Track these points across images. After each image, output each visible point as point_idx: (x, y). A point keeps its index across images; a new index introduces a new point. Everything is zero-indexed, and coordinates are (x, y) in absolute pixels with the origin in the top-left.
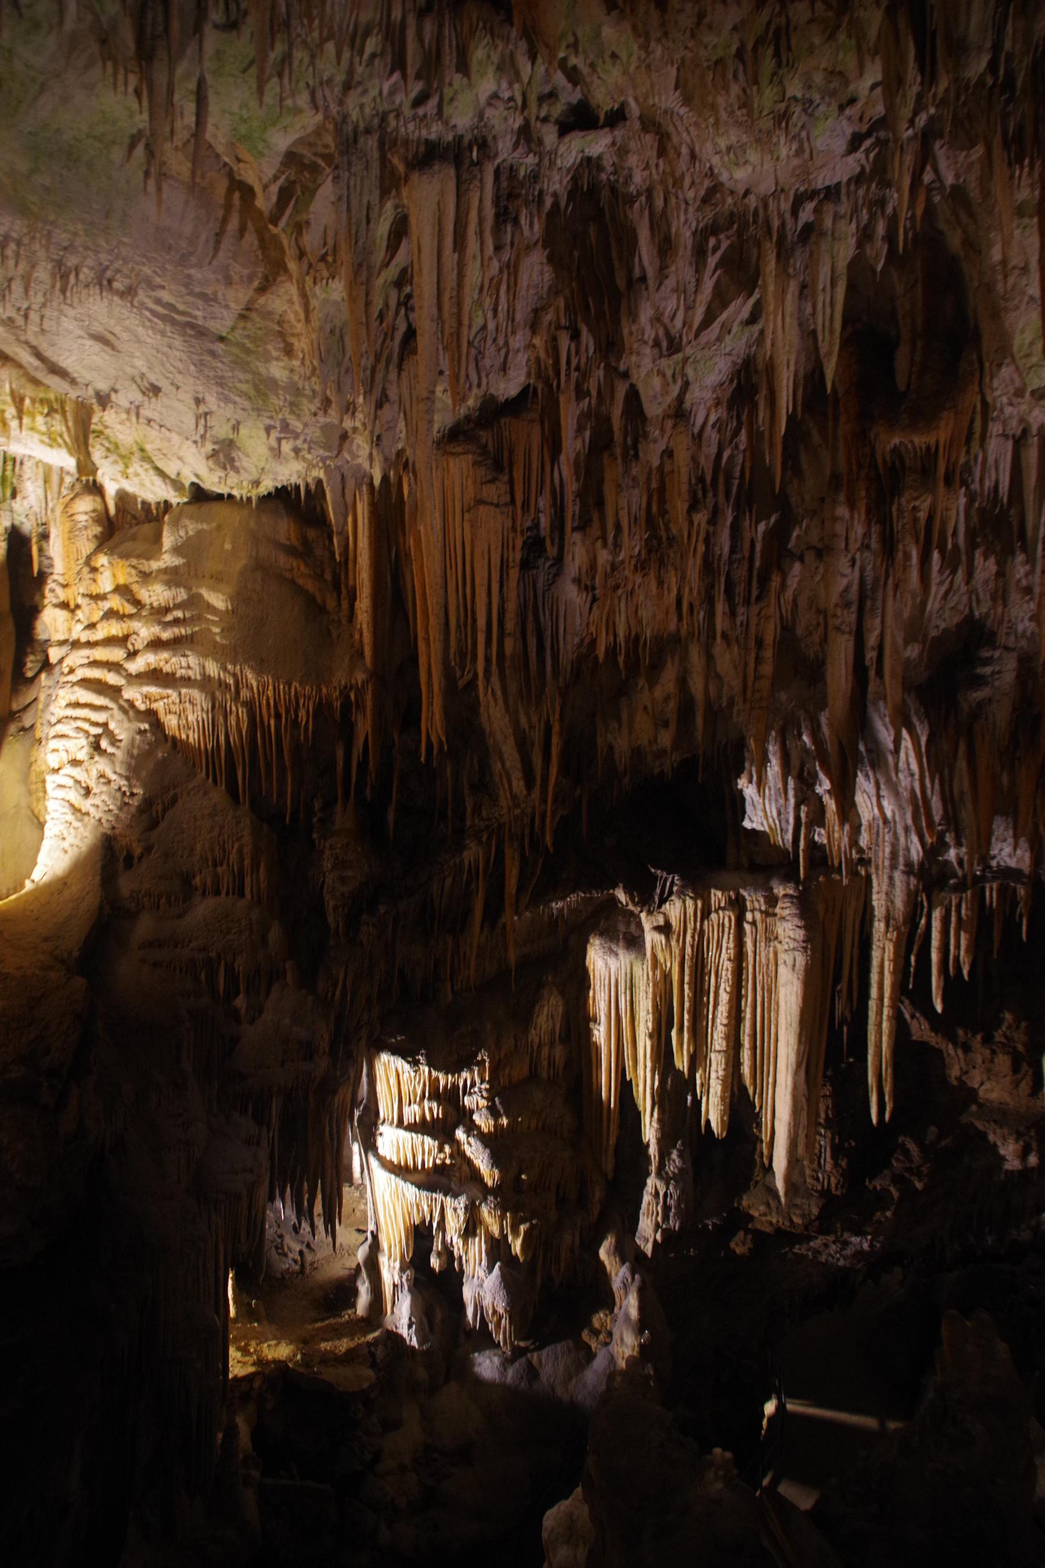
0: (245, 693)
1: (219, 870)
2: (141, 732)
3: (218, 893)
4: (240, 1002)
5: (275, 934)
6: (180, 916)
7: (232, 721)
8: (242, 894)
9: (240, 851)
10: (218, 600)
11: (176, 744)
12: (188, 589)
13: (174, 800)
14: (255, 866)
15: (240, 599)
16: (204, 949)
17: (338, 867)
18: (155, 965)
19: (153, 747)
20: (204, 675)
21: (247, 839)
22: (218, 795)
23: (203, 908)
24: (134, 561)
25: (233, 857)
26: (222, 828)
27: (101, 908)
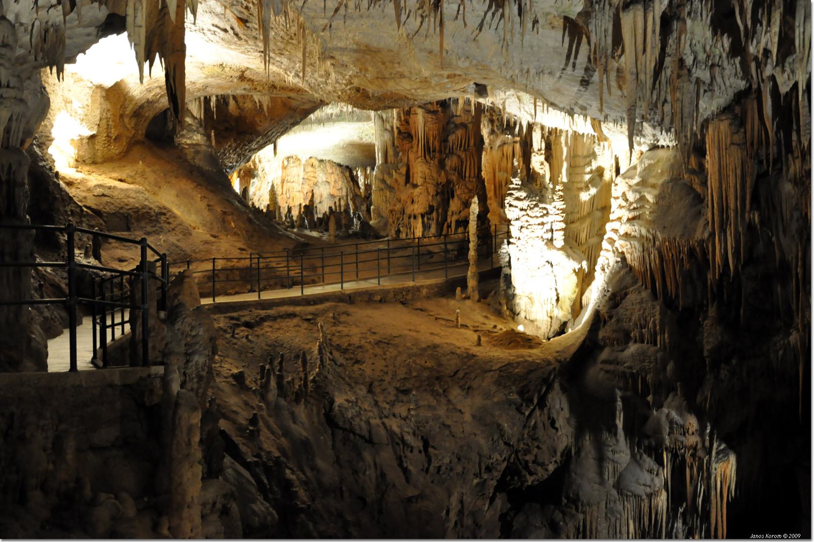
0: (657, 243)
1: (644, 330)
2: (617, 262)
3: (643, 342)
4: (650, 398)
5: (670, 367)
6: (622, 351)
7: (652, 256)
8: (655, 344)
9: (654, 322)
10: (650, 198)
11: (631, 268)
12: (640, 193)
13: (626, 294)
14: (662, 332)
15: (659, 198)
16: (630, 367)
17: (710, 335)
18: (607, 372)
19: (621, 269)
20: (641, 234)
21: (658, 317)
22: (645, 294)
23: (633, 348)
24: (627, 180)
25: (651, 325)
26: (645, 310)
27: (584, 341)
